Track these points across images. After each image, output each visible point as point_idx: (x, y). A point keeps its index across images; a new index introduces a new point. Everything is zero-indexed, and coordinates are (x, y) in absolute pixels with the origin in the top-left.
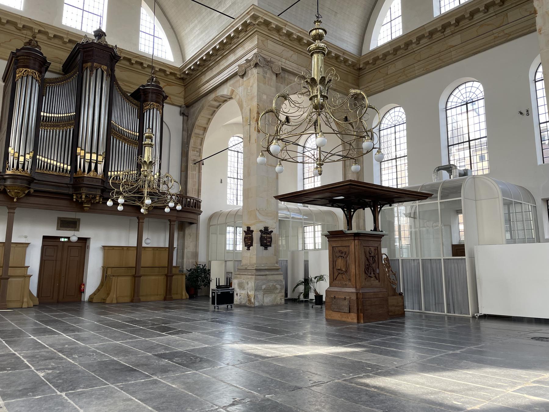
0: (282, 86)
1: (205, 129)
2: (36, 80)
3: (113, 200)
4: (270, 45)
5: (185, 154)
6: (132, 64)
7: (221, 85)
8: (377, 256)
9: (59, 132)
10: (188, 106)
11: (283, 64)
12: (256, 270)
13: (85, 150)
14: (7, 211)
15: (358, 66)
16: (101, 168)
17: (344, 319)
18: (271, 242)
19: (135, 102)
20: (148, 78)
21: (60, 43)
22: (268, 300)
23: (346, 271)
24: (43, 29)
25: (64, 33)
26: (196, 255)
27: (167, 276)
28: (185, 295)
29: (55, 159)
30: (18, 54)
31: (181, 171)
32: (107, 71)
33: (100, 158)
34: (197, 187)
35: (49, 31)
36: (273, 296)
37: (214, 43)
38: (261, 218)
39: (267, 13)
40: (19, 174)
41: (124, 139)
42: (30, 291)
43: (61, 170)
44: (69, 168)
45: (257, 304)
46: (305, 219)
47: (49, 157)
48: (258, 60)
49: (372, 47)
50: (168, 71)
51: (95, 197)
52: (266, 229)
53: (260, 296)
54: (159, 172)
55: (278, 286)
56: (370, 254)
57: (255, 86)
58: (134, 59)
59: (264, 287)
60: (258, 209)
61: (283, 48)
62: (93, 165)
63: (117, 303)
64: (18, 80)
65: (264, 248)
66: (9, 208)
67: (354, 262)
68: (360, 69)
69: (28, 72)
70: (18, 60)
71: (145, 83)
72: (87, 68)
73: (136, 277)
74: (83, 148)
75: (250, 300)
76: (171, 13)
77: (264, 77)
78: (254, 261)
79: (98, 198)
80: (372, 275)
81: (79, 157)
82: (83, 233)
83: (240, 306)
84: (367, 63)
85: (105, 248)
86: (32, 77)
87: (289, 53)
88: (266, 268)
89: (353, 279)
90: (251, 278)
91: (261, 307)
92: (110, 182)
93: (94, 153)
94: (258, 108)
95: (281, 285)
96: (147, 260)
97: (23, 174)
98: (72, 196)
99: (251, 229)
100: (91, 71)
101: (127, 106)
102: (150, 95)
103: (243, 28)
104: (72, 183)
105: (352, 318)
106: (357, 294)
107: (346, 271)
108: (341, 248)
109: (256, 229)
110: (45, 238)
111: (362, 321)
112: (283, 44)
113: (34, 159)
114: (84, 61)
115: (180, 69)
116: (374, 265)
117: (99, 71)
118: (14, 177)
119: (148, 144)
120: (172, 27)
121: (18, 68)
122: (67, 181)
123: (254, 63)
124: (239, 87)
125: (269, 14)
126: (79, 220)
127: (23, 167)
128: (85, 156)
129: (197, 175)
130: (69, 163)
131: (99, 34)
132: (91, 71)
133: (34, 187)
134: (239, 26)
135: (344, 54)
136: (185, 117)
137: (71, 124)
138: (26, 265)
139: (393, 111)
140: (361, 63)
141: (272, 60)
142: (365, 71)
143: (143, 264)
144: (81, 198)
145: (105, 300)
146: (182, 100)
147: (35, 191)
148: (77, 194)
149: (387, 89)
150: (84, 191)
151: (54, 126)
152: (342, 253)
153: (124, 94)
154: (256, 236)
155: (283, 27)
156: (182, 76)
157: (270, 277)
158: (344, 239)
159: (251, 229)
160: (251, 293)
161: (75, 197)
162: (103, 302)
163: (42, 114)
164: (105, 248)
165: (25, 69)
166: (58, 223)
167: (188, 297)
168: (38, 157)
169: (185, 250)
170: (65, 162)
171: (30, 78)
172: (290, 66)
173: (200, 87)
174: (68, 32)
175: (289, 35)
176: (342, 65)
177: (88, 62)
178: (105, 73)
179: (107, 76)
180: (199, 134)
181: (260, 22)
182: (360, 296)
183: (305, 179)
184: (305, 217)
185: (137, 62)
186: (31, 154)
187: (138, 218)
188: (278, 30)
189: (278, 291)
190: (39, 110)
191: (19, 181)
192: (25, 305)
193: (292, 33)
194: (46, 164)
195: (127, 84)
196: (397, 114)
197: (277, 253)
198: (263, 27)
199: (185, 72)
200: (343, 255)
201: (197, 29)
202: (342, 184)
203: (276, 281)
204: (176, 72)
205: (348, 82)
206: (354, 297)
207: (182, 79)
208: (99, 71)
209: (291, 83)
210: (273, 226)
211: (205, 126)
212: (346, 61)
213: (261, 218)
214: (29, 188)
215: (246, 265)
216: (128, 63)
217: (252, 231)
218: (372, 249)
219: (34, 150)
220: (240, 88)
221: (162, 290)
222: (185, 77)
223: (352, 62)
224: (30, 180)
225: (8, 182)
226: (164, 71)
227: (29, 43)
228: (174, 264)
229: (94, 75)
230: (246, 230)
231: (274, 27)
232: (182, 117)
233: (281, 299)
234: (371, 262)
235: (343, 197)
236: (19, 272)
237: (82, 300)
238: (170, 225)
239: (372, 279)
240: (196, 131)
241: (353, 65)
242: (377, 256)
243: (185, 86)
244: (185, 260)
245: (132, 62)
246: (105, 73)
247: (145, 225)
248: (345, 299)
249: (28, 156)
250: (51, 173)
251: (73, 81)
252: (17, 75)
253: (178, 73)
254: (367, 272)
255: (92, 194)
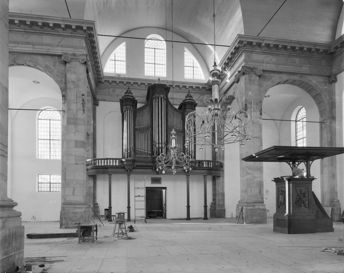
7: (229, 90)
8: (307, 193)
11: (264, 67)
15: (329, 52)
48: (244, 70)
60: (247, 166)
61: (264, 56)
68: (332, 53)
77: (250, 80)
84: (337, 48)
92: (157, 159)
103: (235, 51)
123: (242, 73)
141: (255, 66)
142: (336, 54)
155: (262, 42)
172: (269, 67)
175: (268, 46)
176: (314, 55)
183: (297, 140)
188: (259, 45)
195: (179, 100)
202: (268, 150)
212: (318, 50)
213: (249, 172)
235: (284, 156)
241: (325, 52)
242: (307, 193)
247: (207, 179)
254: (297, 203)
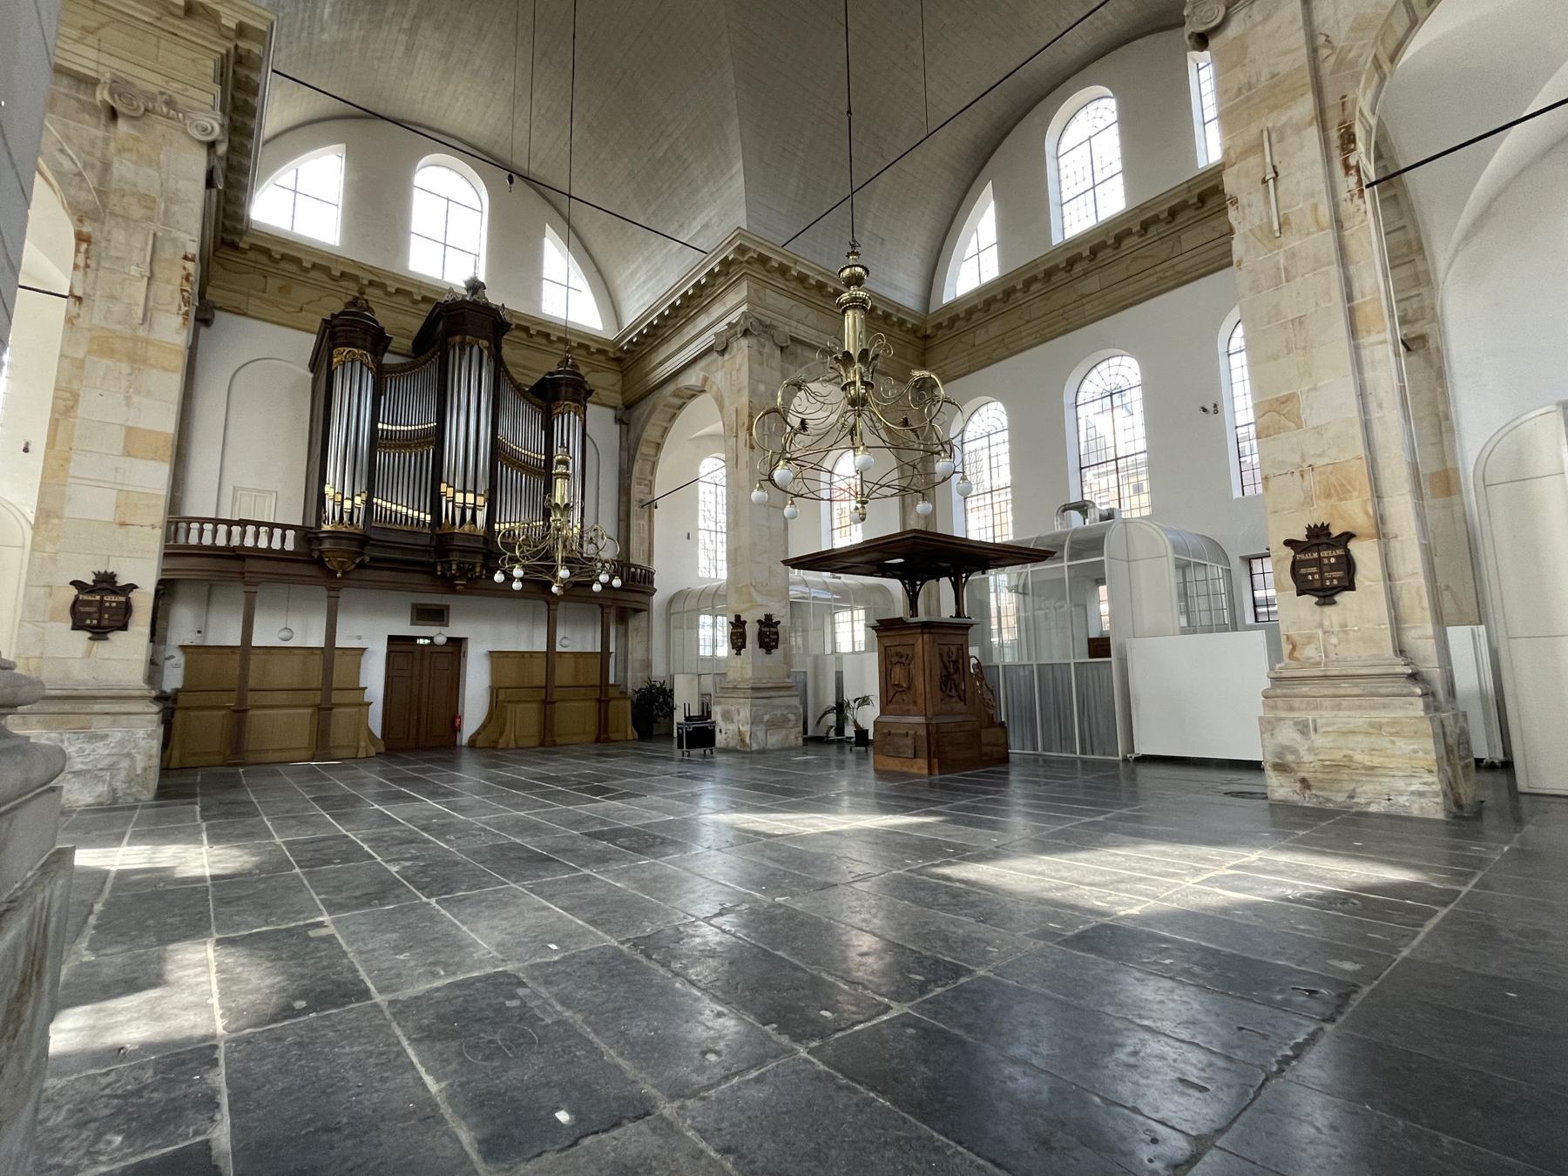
0: (792, 368)
1: (659, 447)
2: (369, 368)
3: (504, 572)
4: (770, 297)
5: (624, 491)
6: (532, 336)
8: (961, 661)
9: (410, 457)
10: (629, 406)
11: (793, 330)
12: (753, 689)
13: (454, 487)
14: (325, 593)
15: (923, 332)
16: (481, 516)
17: (905, 769)
18: (777, 640)
19: (538, 401)
20: (559, 360)
21: (407, 302)
22: (774, 740)
23: (909, 688)
24: (376, 279)
25: (413, 285)
26: (647, 665)
27: (599, 701)
28: (631, 733)
29: (405, 504)
30: (335, 322)
31: (619, 520)
32: (488, 349)
33: (480, 501)
34: (646, 548)
35: (388, 283)
36: (784, 732)
37: (672, 295)
38: (759, 599)
39: (762, 241)
40: (344, 529)
41: (520, 467)
42: (369, 729)
43: (415, 522)
44: (428, 518)
45: (755, 747)
46: (836, 600)
47: (394, 501)
49: (947, 299)
50: (594, 347)
51: (474, 568)
52: (769, 617)
53: (761, 734)
54: (582, 522)
55: (792, 717)
56: (949, 657)
57: (745, 368)
58: (535, 327)
59: (766, 718)
61: (792, 302)
62: (469, 513)
63: (517, 748)
64: (336, 368)
65: (764, 651)
66: (329, 589)
67: (921, 673)
68: (926, 337)
69: (354, 354)
70: (335, 333)
71: (554, 368)
72: (454, 346)
73: (547, 703)
74: (451, 483)
75: (743, 741)
76: (597, 247)
77: (760, 353)
78: (749, 673)
79: (478, 569)
80: (954, 693)
81: (444, 499)
82: (456, 629)
83: (726, 751)
84: (939, 326)
85: (494, 656)
86: (361, 363)
87: (802, 311)
88: (770, 685)
89: (921, 701)
90: (745, 703)
91: (763, 752)
93: (470, 492)
94: (750, 407)
95: (795, 714)
96: (564, 675)
97: (351, 530)
98: (435, 566)
99: (742, 619)
100: (462, 350)
101: (524, 407)
102: (563, 389)
104: (434, 543)
105: (920, 766)
106: (927, 725)
107: (909, 688)
108: (898, 649)
109: (752, 618)
110: (392, 639)
111: (937, 772)
112: (793, 296)
113: (369, 503)
114: (449, 333)
115: (615, 343)
116: (956, 676)
117: (475, 350)
118: (334, 535)
119: (562, 474)
120: (599, 271)
121: (336, 346)
122: (426, 541)
124: (717, 370)
125: (766, 243)
126: (448, 607)
127: (351, 519)
128: (454, 497)
129: (646, 527)
130: (428, 511)
131: (475, 286)
132: (462, 350)
133: (370, 553)
134: (715, 265)
135: (898, 310)
136: (624, 427)
137: (429, 443)
138: (361, 686)
139: (985, 408)
140: (929, 325)
141: (774, 322)
143: (558, 682)
144: (450, 569)
145: (496, 742)
146: (619, 396)
147: (373, 559)
148: (442, 563)
149: (973, 372)
150: (455, 557)
151: (401, 446)
152: (901, 657)
153: (518, 388)
154: (751, 631)
155: (791, 265)
156: (618, 354)
157: (777, 701)
158: (904, 632)
159: (742, 619)
160: (746, 729)
161: (439, 568)
162: (493, 746)
163: (380, 426)
164: (494, 656)
165: (347, 349)
166: (412, 613)
167: (636, 735)
168: (375, 500)
169: (630, 657)
170: (422, 509)
171: (358, 365)
172: (804, 333)
173: (648, 374)
174: (420, 284)
175: (802, 279)
177: (455, 335)
178: (486, 352)
179: (489, 357)
180: (647, 455)
181: (752, 257)
182: (933, 730)
184: (835, 596)
185: (539, 333)
186: (364, 496)
187: (548, 603)
188: (783, 270)
189: (791, 724)
190: (375, 419)
191: (344, 542)
192: (362, 754)
193: (807, 277)
194: (388, 512)
196: (992, 413)
197: (788, 659)
198: (757, 266)
199: (622, 347)
200: (903, 660)
201: (642, 272)
203: (788, 707)
204: (606, 349)
205: (906, 359)
206: (922, 732)
207: (617, 360)
208: (475, 349)
209: (807, 363)
210: (780, 612)
211: (658, 441)
212: (902, 322)
213: (759, 599)
214: (362, 554)
215: (735, 681)
216: (523, 335)
217: (745, 622)
218: (954, 649)
219: (368, 489)
220: (720, 373)
221: (591, 727)
222: (623, 356)
223: (913, 325)
224: (363, 541)
225: (327, 545)
226: (586, 347)
227: (354, 303)
228: (612, 681)
229: (467, 357)
230: (733, 620)
231: (777, 265)
232: (618, 426)
233: (796, 738)
234: (952, 671)
236: (350, 697)
237: (458, 742)
238: (602, 614)
239: (953, 700)
240: (644, 449)
241: (915, 330)
242: (961, 661)
243: (624, 372)
244: (629, 674)
245: (532, 332)
246: (486, 352)
247: (559, 615)
248: (907, 734)
249: (358, 500)
250: (398, 527)
251: (432, 370)
252: (335, 360)
253: (610, 350)
255: (470, 563)
